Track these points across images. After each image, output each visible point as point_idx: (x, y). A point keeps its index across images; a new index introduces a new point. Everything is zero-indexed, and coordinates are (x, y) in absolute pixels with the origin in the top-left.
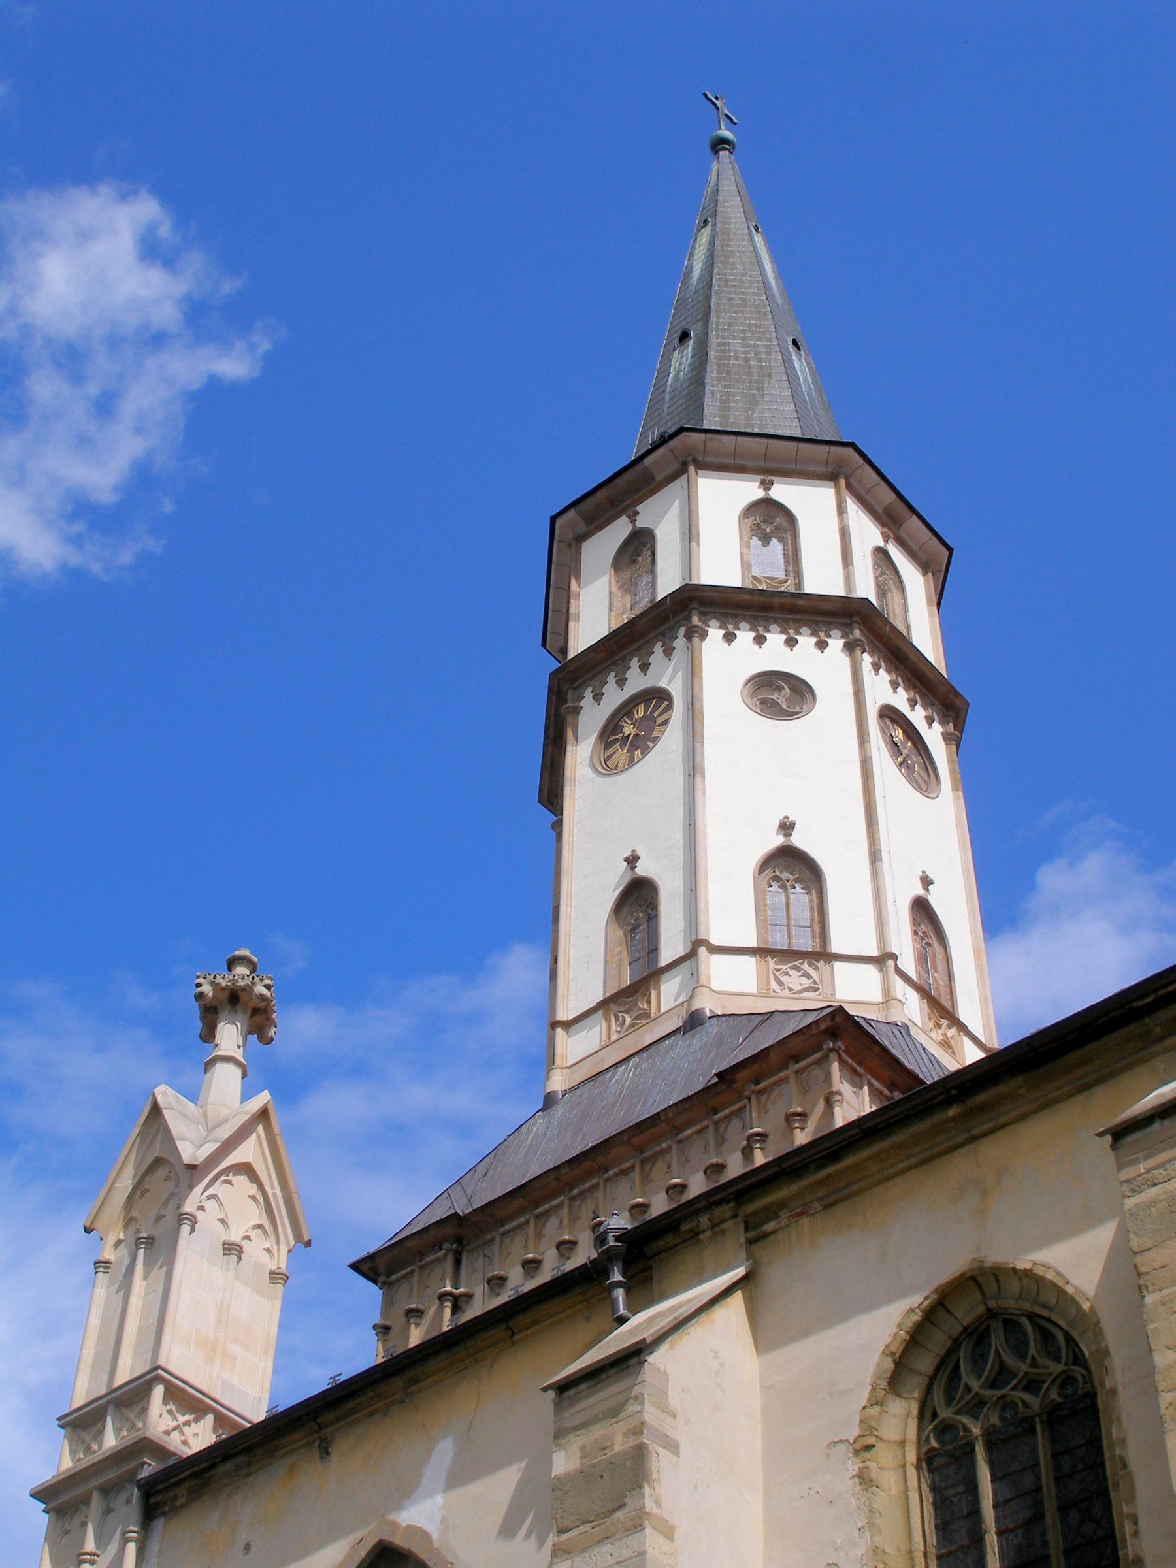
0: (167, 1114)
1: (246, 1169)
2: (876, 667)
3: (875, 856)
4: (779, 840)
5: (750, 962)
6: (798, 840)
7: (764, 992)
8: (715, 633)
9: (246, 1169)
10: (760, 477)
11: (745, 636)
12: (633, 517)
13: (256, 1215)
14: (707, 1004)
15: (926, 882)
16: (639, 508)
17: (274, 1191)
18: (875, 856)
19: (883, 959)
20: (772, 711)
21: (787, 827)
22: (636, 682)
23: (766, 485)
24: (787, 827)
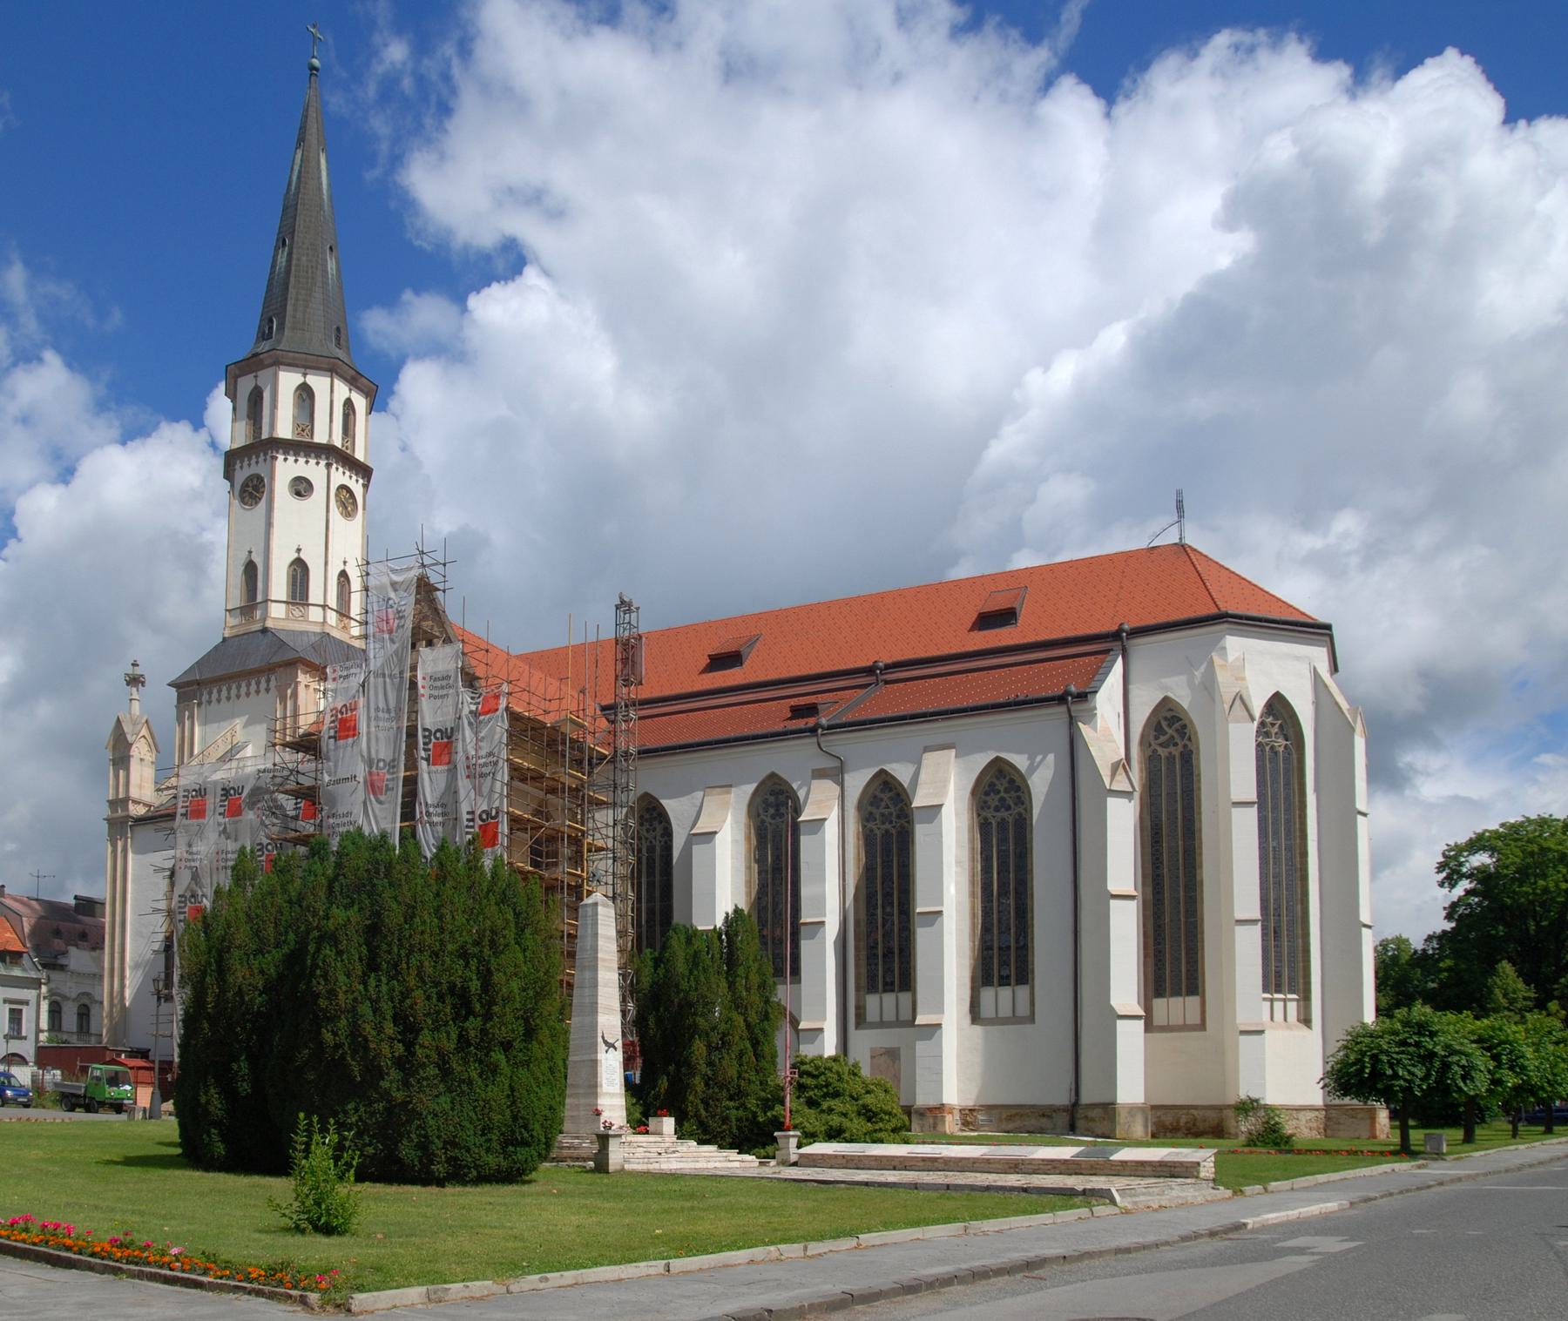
0: (123, 724)
1: (144, 736)
2: (337, 469)
3: (326, 563)
4: (296, 555)
5: (283, 605)
6: (303, 556)
7: (287, 618)
8: (281, 457)
9: (144, 736)
10: (303, 370)
11: (291, 459)
12: (256, 377)
13: (147, 748)
14: (269, 624)
15: (345, 563)
16: (259, 373)
17: (150, 740)
18: (326, 563)
19: (324, 607)
20: (298, 494)
21: (299, 550)
22: (254, 470)
23: (305, 375)
24: (299, 550)
